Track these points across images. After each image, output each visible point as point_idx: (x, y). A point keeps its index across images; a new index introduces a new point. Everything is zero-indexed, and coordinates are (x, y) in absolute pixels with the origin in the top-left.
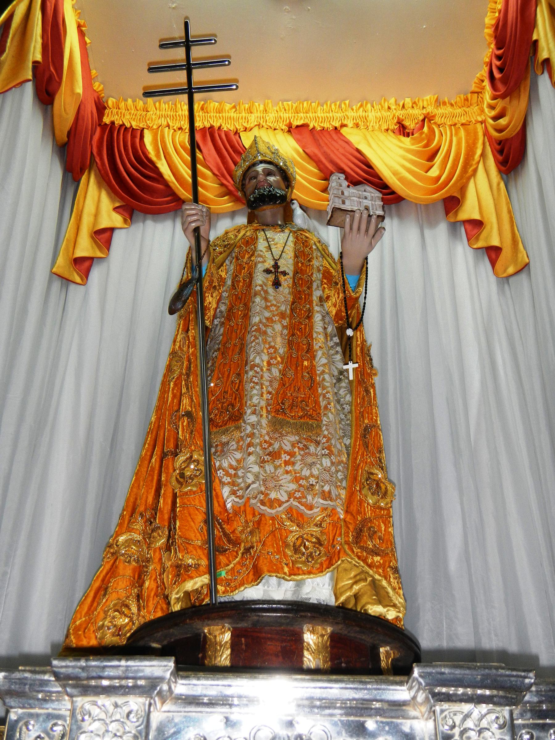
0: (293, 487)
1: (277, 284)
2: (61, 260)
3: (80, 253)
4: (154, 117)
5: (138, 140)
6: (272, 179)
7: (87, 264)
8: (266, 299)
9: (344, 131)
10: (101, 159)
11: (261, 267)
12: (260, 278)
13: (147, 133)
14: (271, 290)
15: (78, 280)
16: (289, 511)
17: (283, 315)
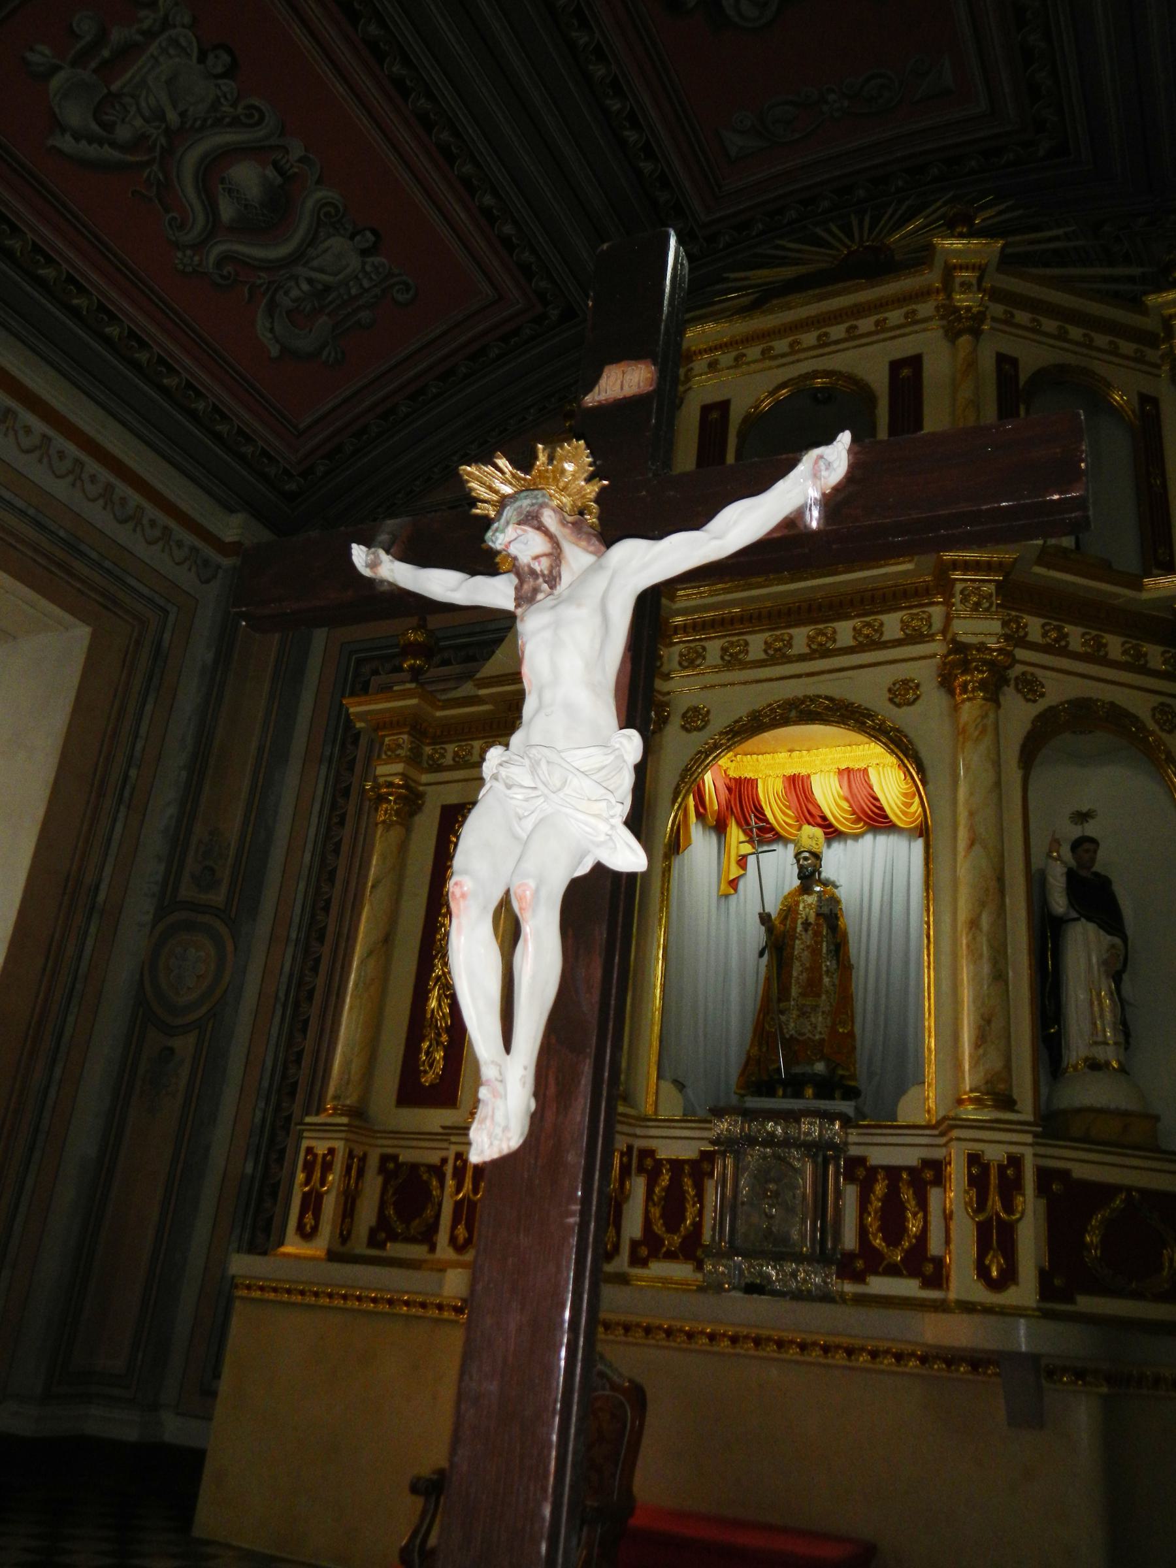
0: (809, 1027)
1: (806, 930)
2: (723, 886)
3: (732, 877)
4: (763, 768)
5: (754, 791)
6: (806, 863)
7: (736, 881)
8: (801, 939)
9: (870, 770)
10: (737, 810)
11: (799, 921)
12: (799, 928)
13: (759, 781)
14: (803, 933)
15: (732, 891)
16: (809, 1038)
17: (808, 947)
